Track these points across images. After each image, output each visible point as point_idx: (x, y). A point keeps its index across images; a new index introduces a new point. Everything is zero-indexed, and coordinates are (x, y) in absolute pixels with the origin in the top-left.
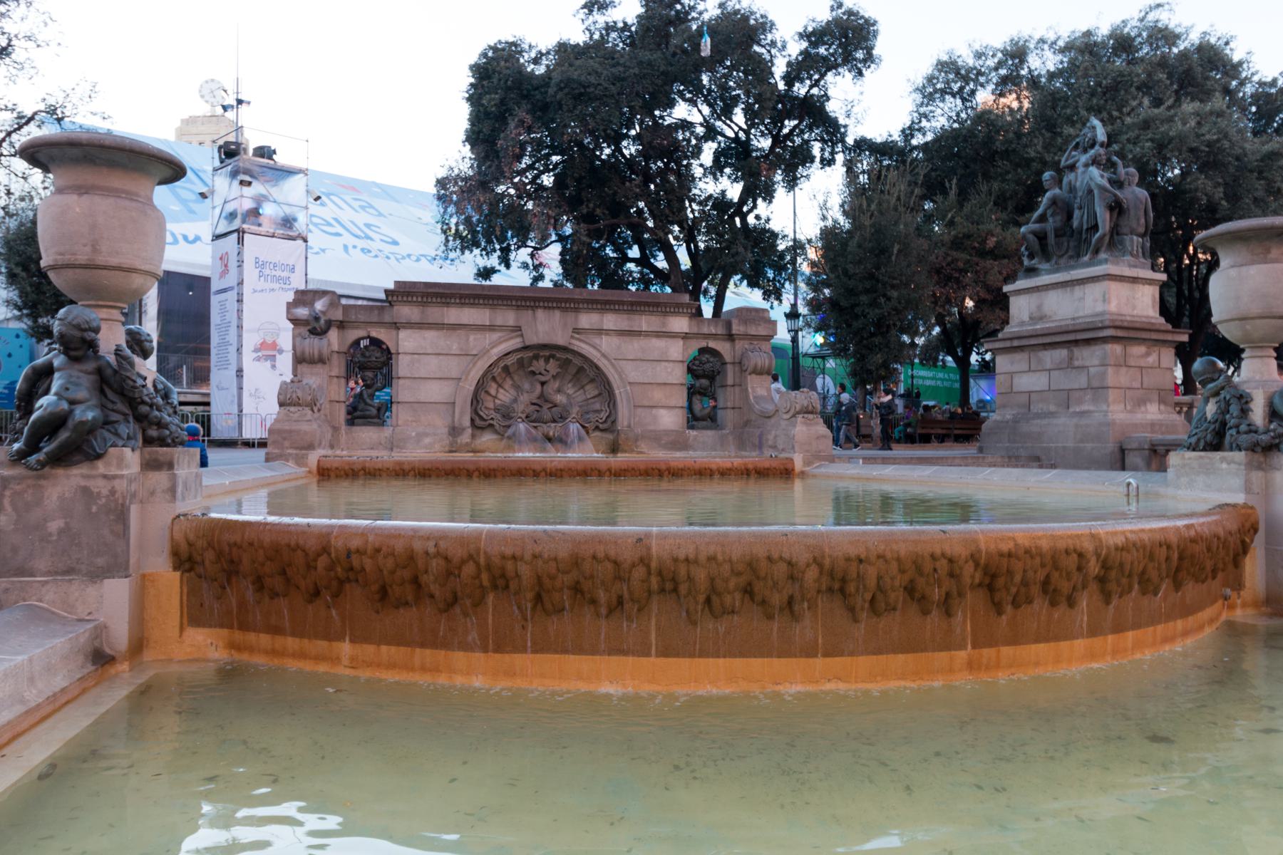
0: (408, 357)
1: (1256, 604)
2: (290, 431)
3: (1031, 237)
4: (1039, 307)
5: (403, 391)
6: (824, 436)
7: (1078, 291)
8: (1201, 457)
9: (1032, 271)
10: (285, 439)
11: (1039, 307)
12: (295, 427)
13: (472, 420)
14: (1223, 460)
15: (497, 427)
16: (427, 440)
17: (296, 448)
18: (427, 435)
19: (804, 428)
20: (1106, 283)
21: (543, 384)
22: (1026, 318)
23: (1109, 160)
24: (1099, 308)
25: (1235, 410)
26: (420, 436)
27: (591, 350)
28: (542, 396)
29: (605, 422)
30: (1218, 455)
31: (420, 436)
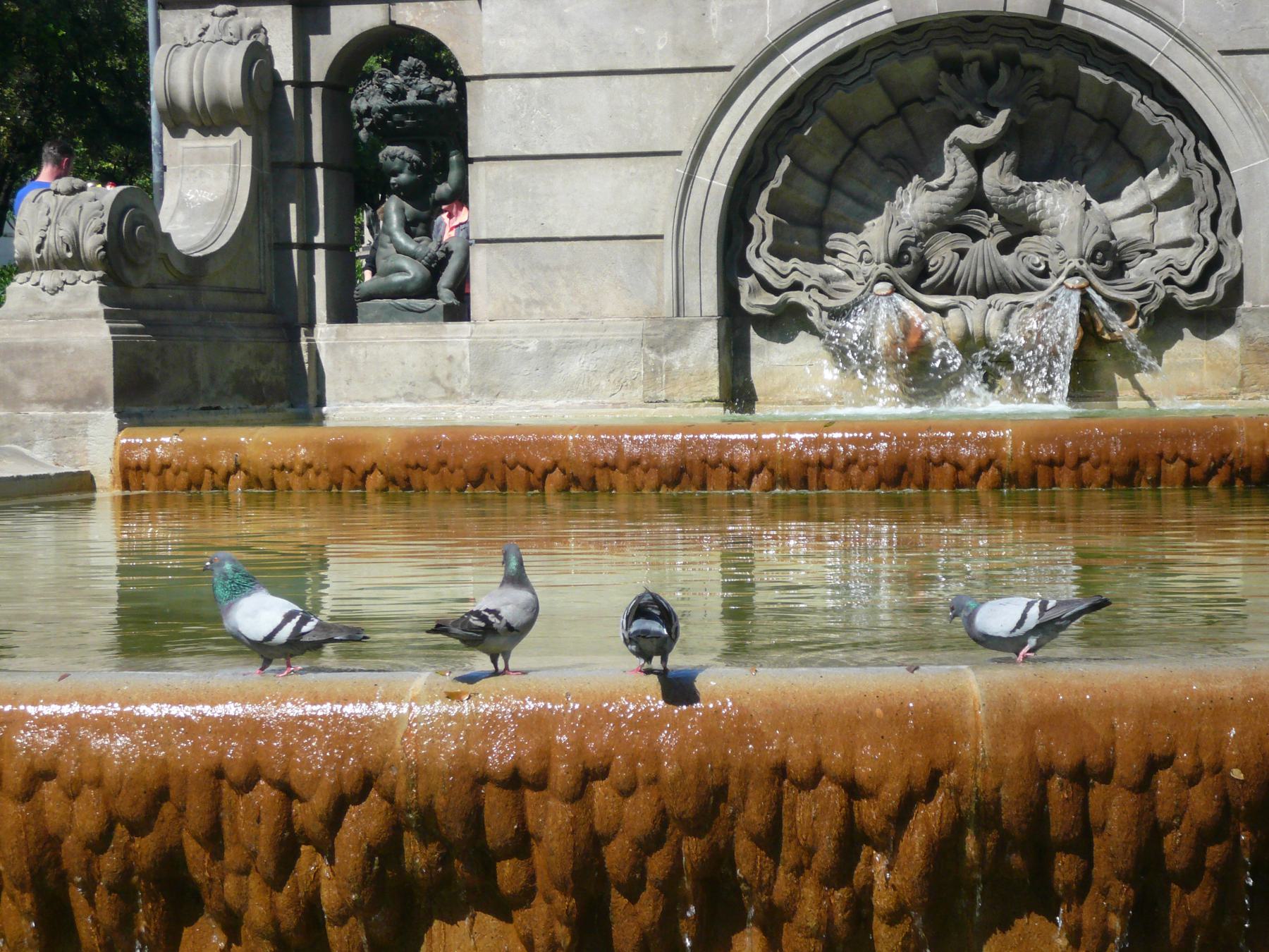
0: (514, 86)
2: (38, 350)
5: (493, 202)
10: (21, 374)
12: (49, 335)
13: (729, 295)
15: (814, 318)
16: (575, 366)
17: (54, 403)
18: (569, 347)
21: (980, 157)
26: (551, 354)
27: (1137, 23)
28: (975, 199)
29: (1200, 285)
31: (551, 354)
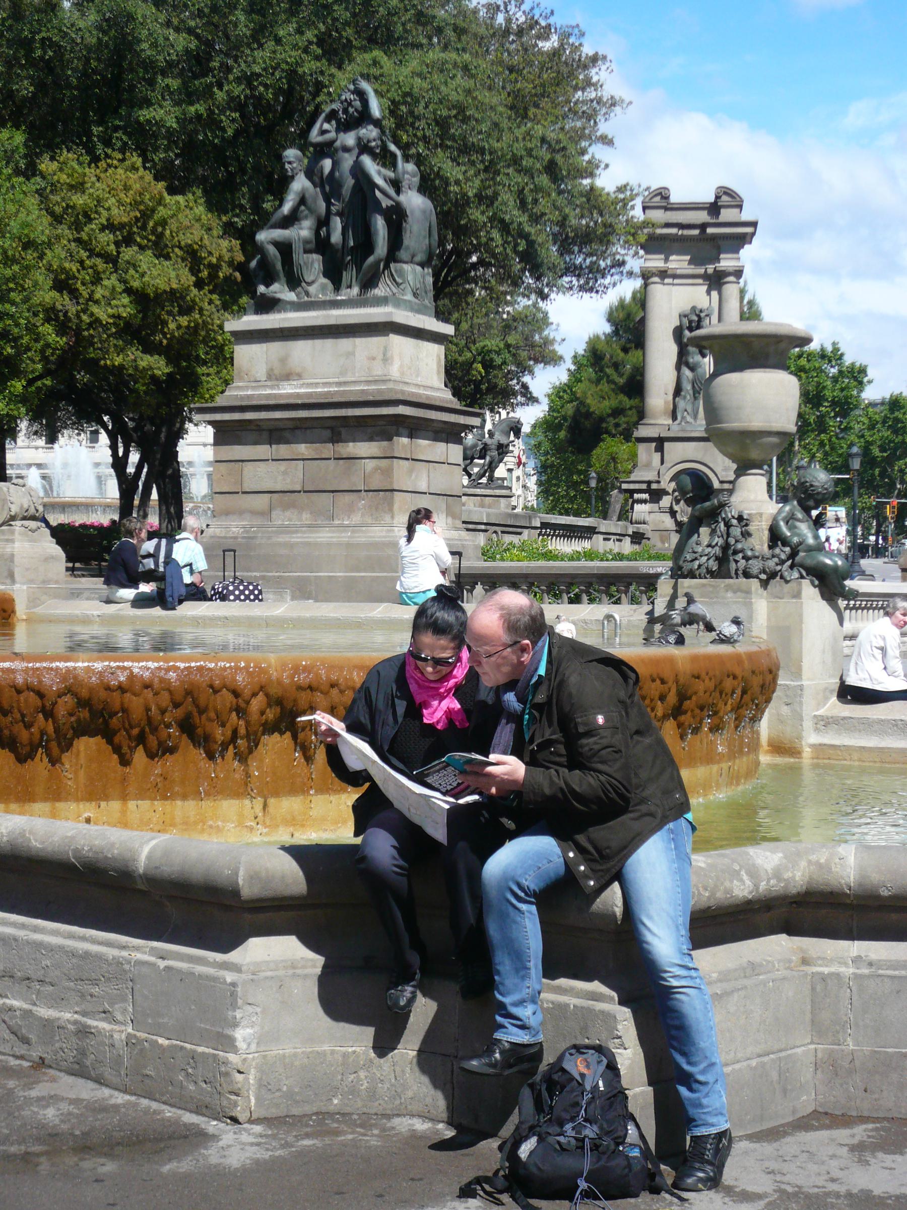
1: (767, 752)
3: (272, 250)
4: (283, 360)
6: (53, 558)
7: (345, 344)
8: (704, 585)
9: (267, 305)
11: (283, 360)
14: (728, 588)
19: (27, 545)
20: (395, 340)
22: (261, 374)
23: (384, 148)
24: (378, 370)
25: (736, 531)
30: (722, 583)
